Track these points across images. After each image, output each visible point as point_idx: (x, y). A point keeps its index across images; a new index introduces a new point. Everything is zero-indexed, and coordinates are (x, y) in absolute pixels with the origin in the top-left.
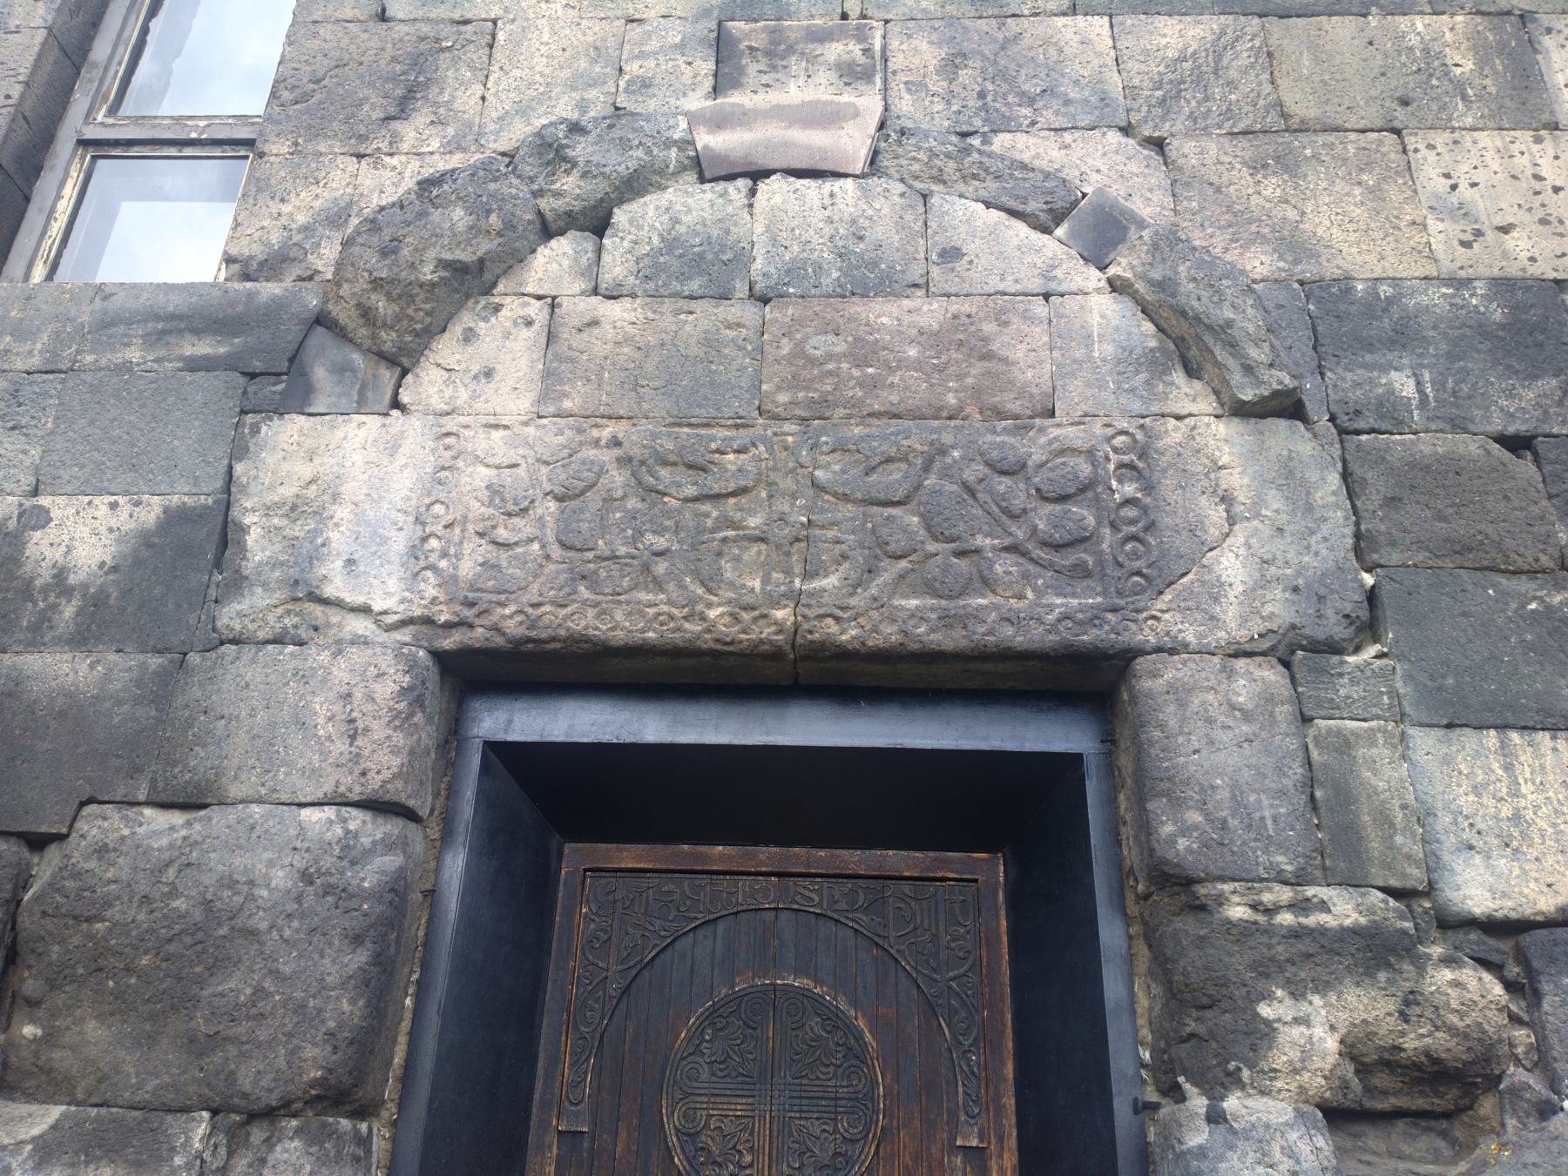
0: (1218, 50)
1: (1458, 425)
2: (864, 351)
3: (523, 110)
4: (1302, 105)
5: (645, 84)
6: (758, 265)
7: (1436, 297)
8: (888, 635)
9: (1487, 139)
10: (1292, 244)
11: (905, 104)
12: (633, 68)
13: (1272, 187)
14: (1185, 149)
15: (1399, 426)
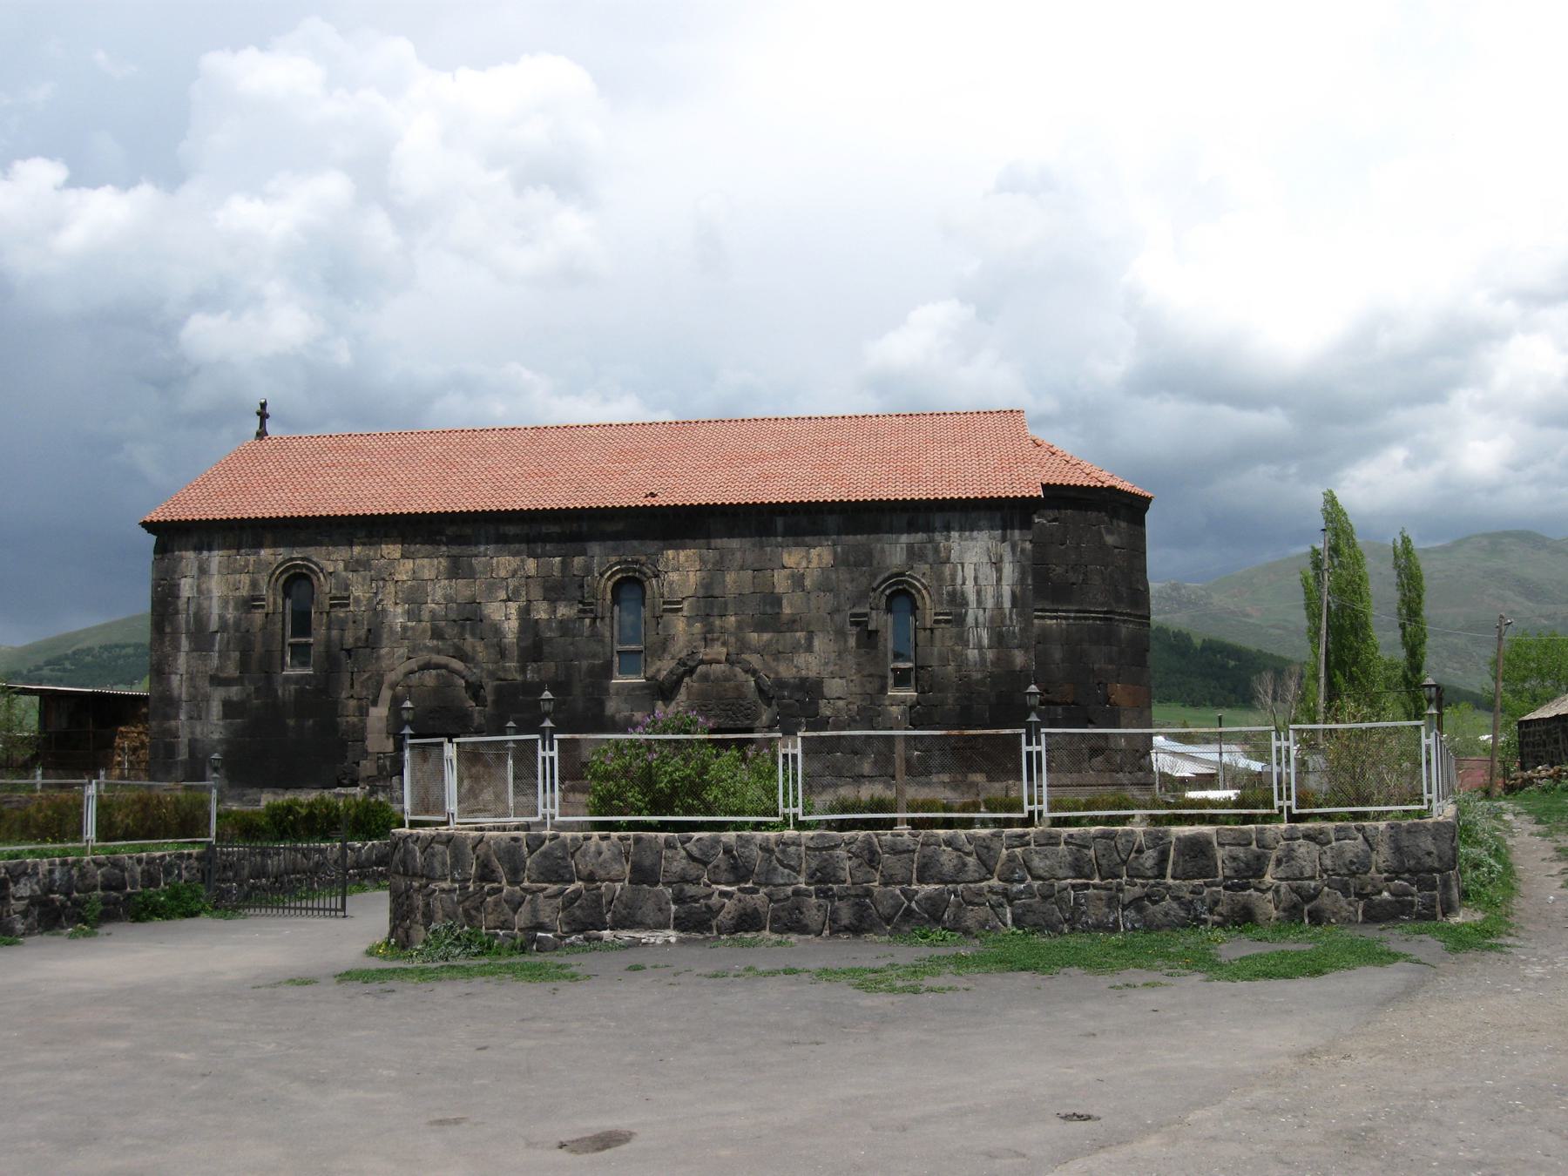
0: (771, 640)
1: (790, 698)
2: (725, 690)
3: (680, 652)
4: (781, 650)
5: (695, 647)
6: (712, 677)
7: (792, 680)
8: (728, 726)
9: (803, 655)
10: (777, 673)
11: (730, 649)
12: (694, 644)
13: (775, 663)
14: (766, 657)
15: (784, 699)
